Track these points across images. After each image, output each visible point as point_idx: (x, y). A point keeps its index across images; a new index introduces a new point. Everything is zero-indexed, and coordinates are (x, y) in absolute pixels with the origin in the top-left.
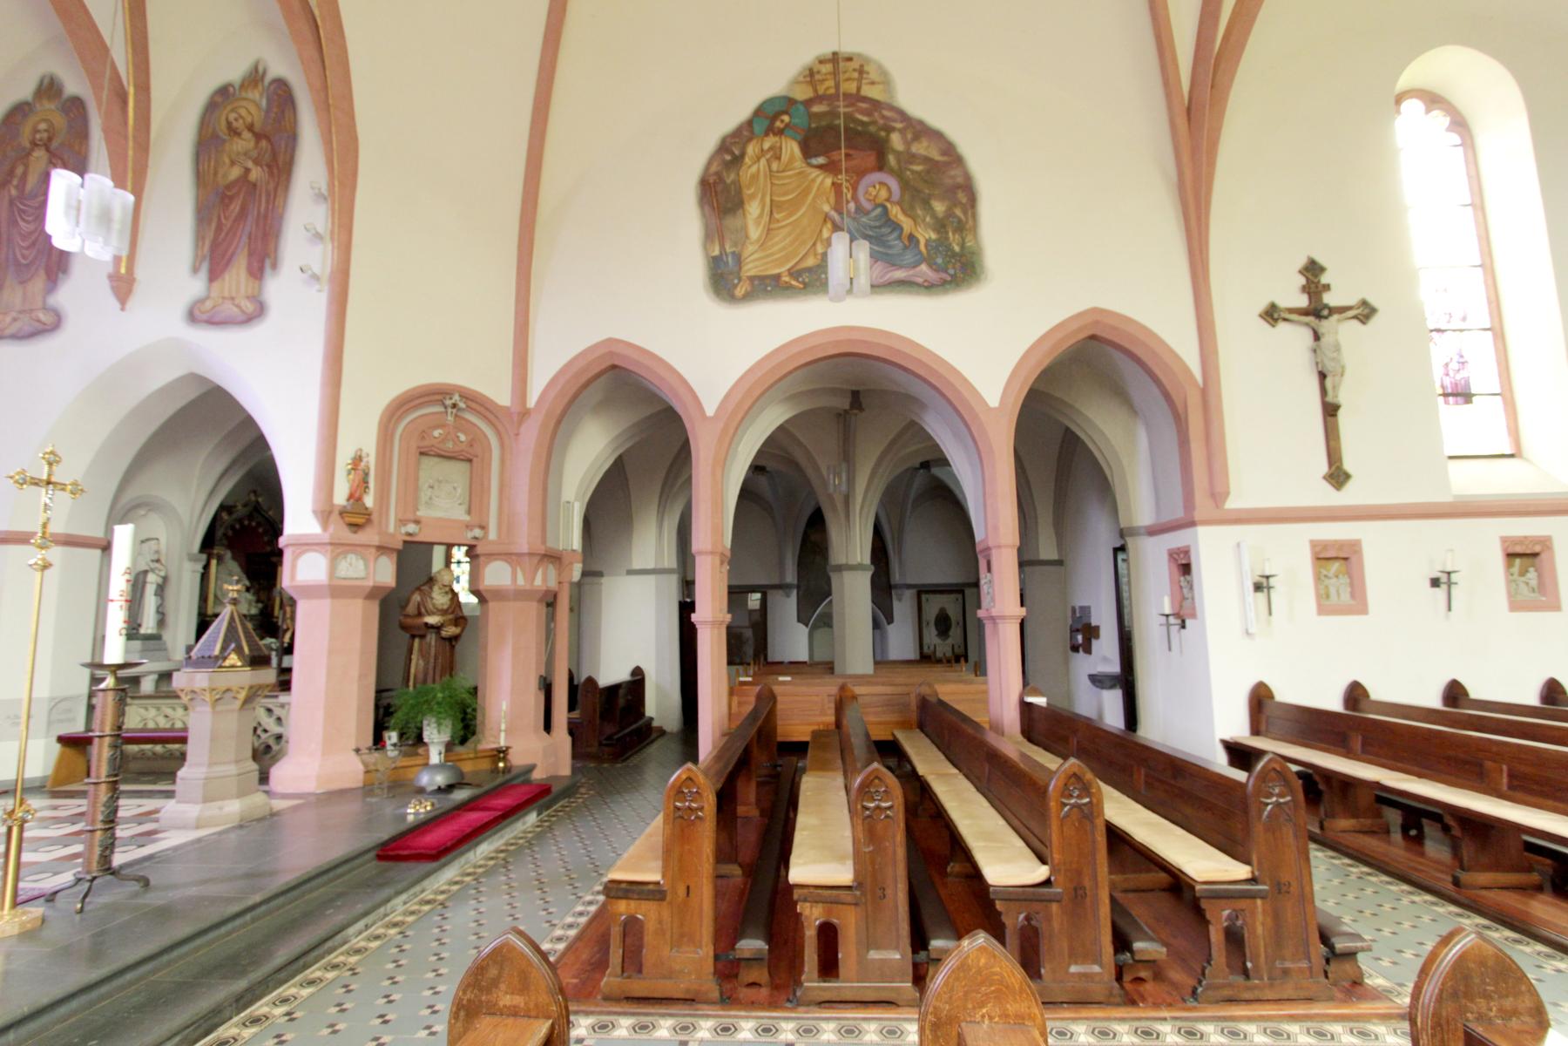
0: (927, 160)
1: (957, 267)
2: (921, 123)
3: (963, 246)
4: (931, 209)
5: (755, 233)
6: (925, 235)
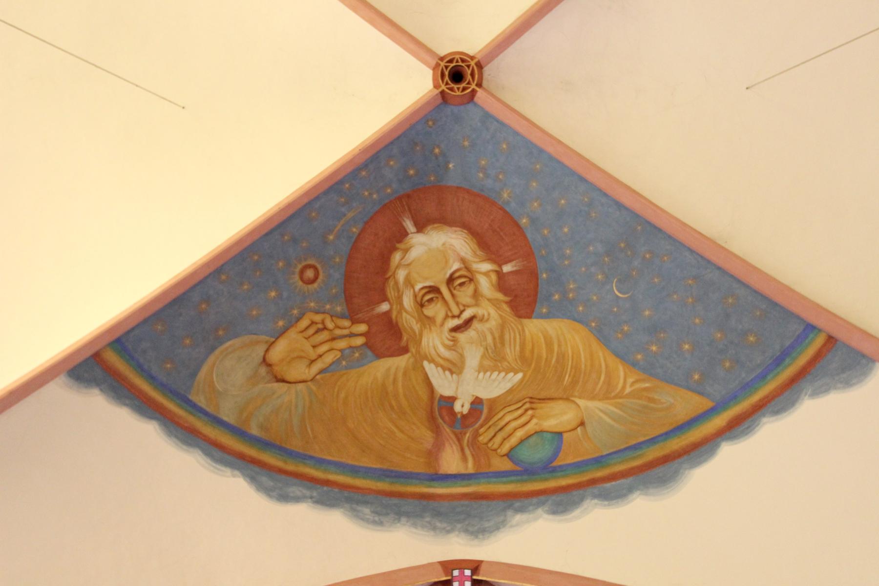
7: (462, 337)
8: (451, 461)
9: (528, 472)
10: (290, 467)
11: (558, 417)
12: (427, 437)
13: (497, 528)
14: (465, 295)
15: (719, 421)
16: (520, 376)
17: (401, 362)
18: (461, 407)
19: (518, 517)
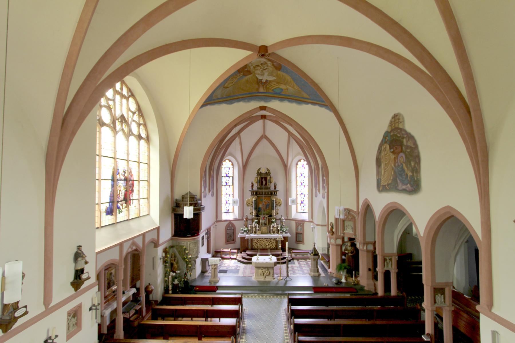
0: (411, 147)
1: (414, 187)
2: (410, 134)
3: (417, 179)
4: (410, 164)
5: (383, 173)
6: (410, 174)
7: (264, 71)
8: (261, 90)
9: (276, 93)
10: (232, 98)
11: (283, 87)
12: (257, 86)
13: (270, 101)
14: (264, 66)
17: (251, 76)
18: (264, 81)
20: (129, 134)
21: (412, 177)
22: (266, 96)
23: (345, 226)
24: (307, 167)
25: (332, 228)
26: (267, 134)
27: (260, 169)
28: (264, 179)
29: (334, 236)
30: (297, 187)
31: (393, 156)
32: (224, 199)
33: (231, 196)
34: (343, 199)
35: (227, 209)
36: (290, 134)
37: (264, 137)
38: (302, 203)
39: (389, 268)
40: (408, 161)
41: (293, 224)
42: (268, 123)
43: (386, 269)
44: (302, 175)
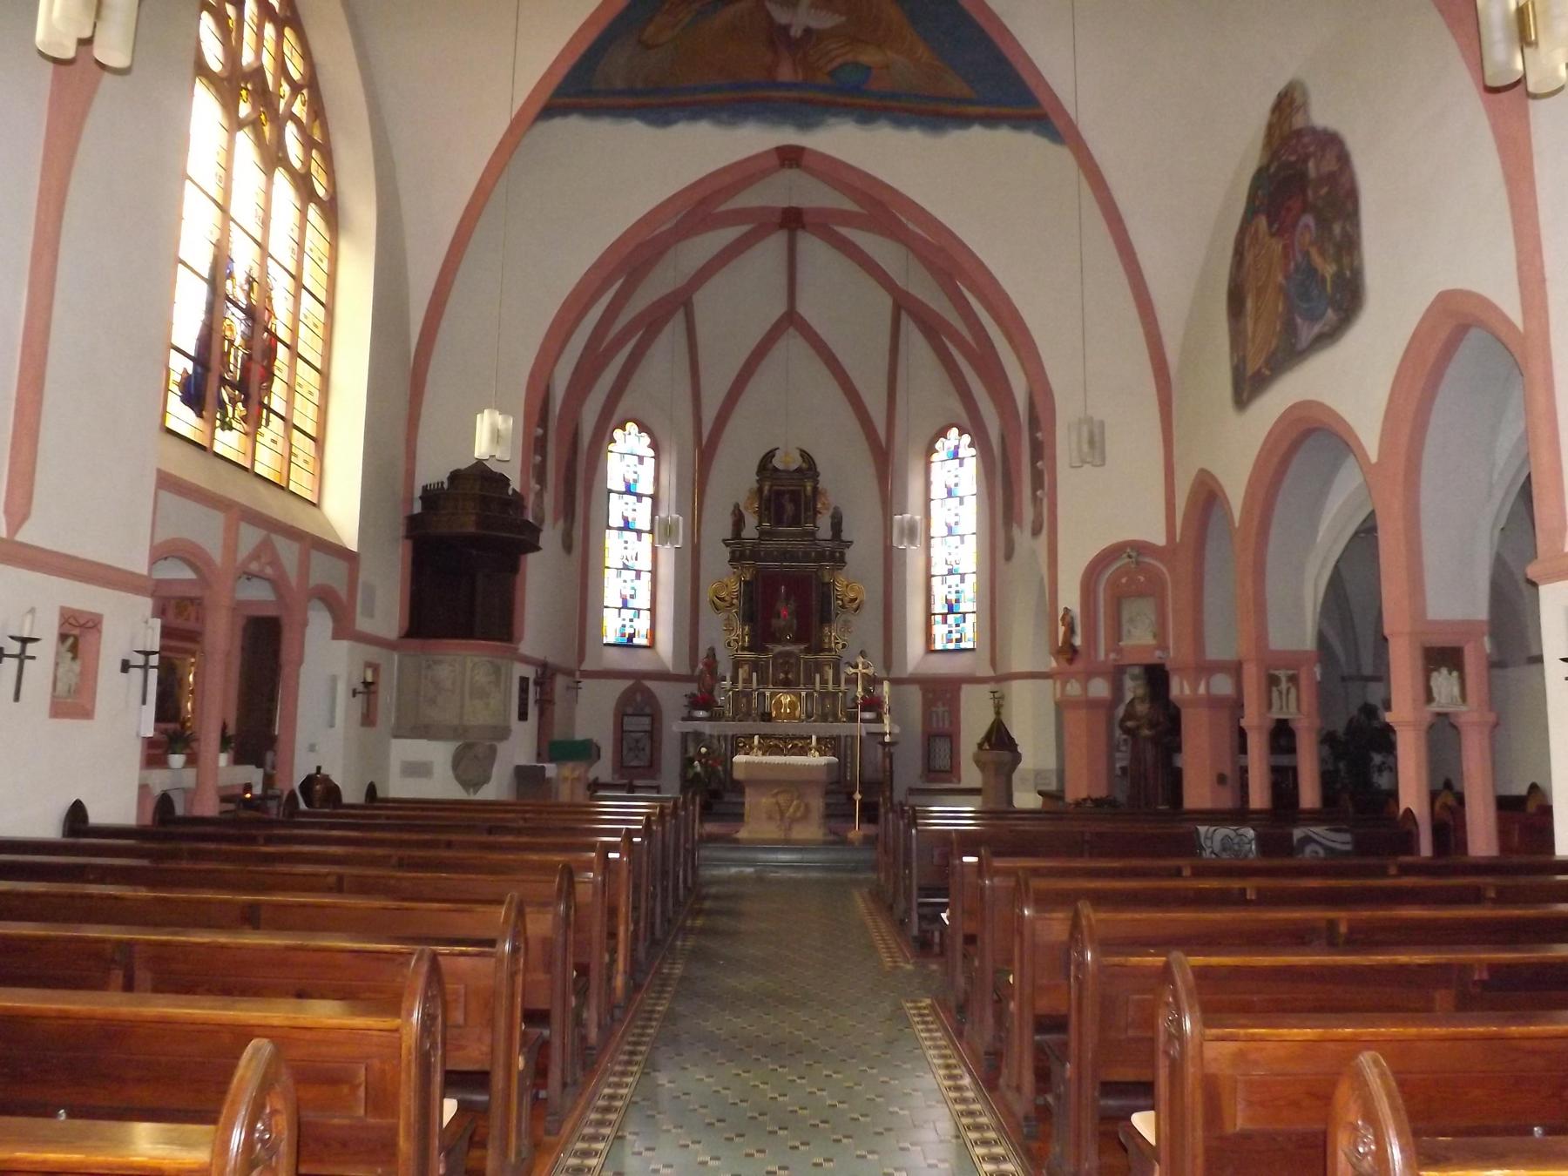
6: (1329, 270)
8: (785, 73)
11: (870, 56)
15: (980, 110)
16: (843, 19)
18: (796, 32)
19: (832, 120)
20: (273, 157)
21: (1339, 275)
22: (802, 101)
23: (1125, 616)
24: (968, 452)
25: (1071, 630)
26: (804, 309)
27: (770, 455)
28: (787, 494)
29: (1079, 665)
30: (928, 547)
31: (1277, 246)
32: (613, 587)
33: (646, 577)
34: (1112, 501)
35: (629, 631)
36: (903, 304)
37: (791, 320)
38: (951, 611)
39: (1290, 713)
40: (1324, 224)
41: (915, 695)
42: (811, 247)
43: (1276, 714)
44: (950, 494)
